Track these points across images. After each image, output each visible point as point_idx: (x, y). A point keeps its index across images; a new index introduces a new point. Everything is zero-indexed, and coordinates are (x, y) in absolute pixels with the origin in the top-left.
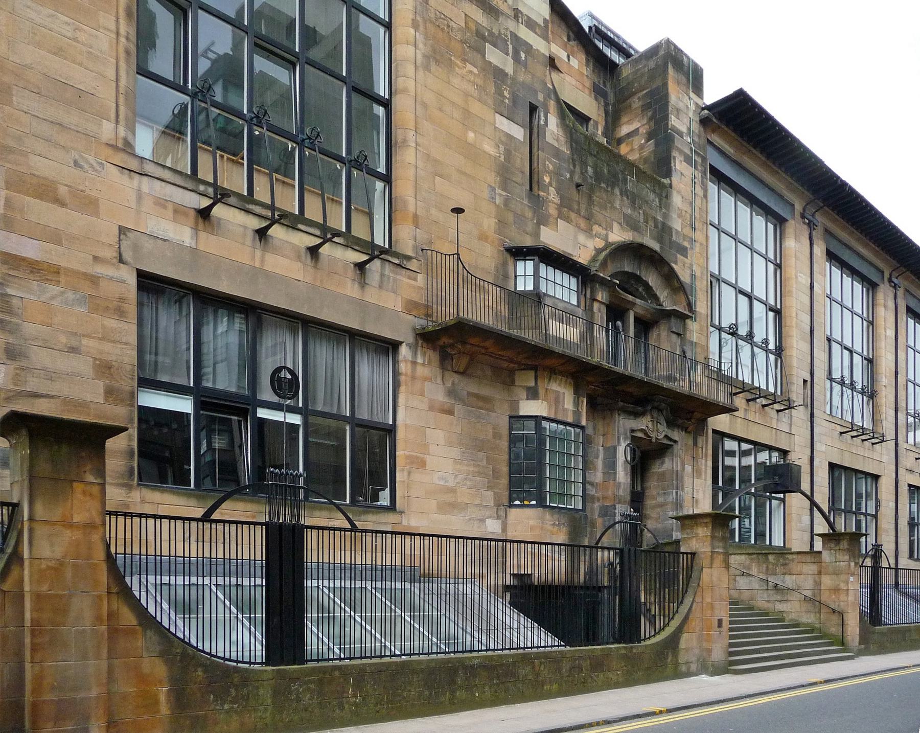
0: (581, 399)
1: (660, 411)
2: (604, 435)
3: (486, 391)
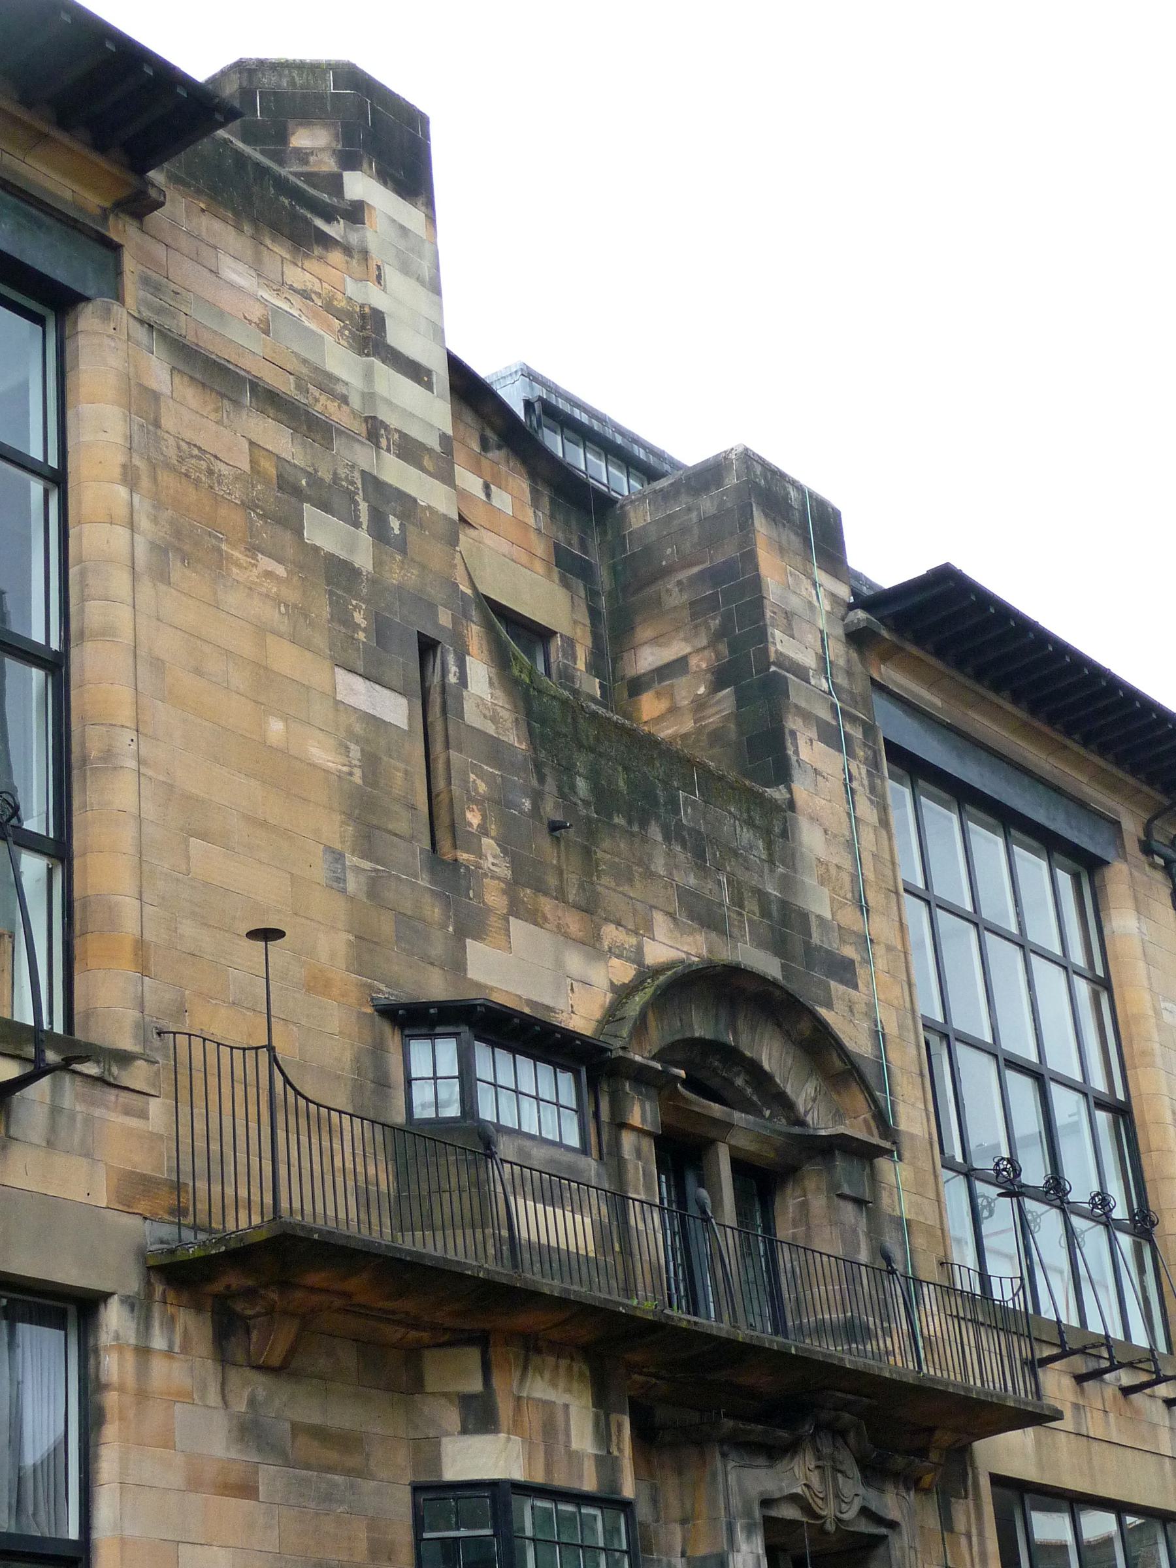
1: (839, 1433)
2: (684, 1521)
3: (344, 1416)
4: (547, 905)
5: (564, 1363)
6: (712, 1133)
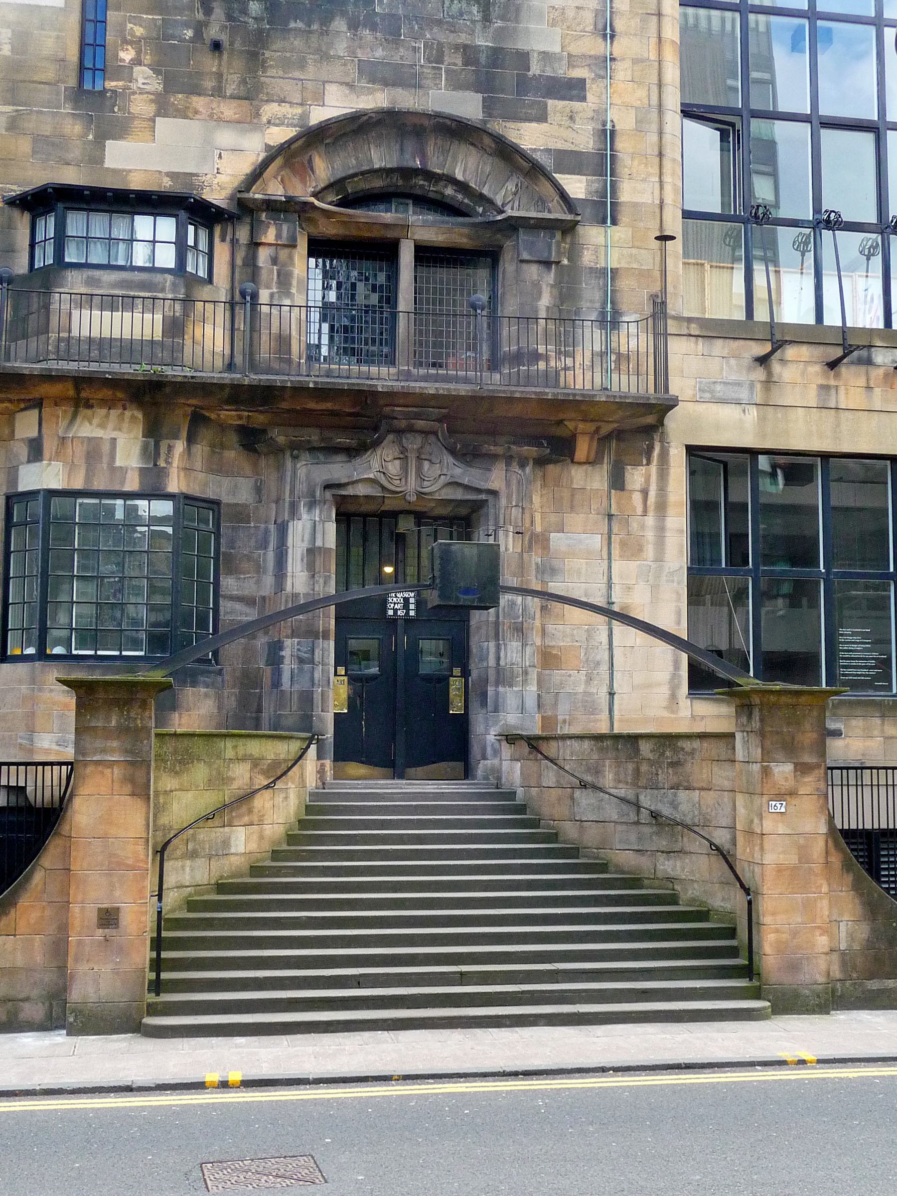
1: (425, 433)
2: (277, 502)
4: (199, 102)
6: (390, 234)
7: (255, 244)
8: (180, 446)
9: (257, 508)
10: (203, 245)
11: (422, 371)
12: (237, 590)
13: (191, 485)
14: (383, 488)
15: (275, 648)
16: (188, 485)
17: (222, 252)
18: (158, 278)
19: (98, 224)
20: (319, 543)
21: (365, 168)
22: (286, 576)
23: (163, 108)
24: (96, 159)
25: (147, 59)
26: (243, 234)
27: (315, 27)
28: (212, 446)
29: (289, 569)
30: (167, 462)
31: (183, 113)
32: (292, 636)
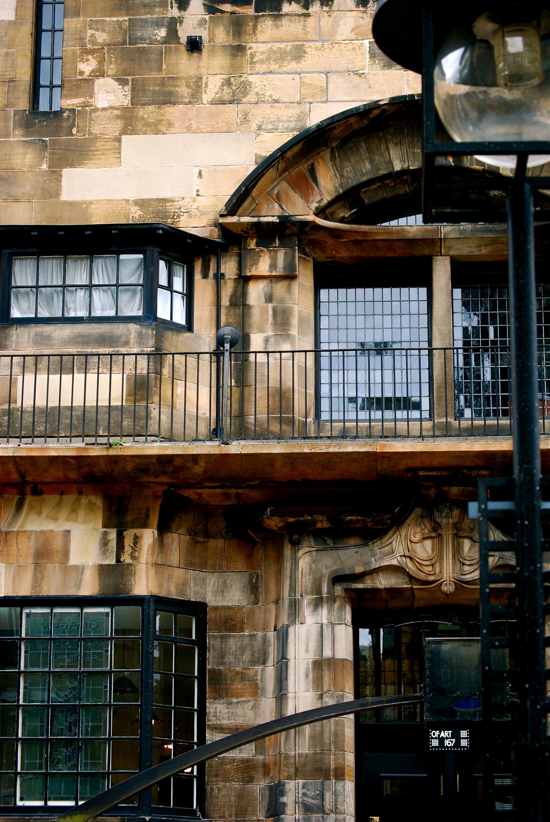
0: (129, 535)
5: (69, 498)
7: (244, 280)
8: (148, 536)
9: (253, 611)
10: (178, 284)
11: (491, 422)
12: (229, 719)
13: (165, 584)
14: (411, 578)
15: (276, 791)
16: (160, 586)
17: (204, 289)
18: (119, 329)
19: (51, 270)
20: (327, 653)
21: (383, 172)
22: (287, 698)
23: (129, 122)
24: (51, 190)
25: (111, 68)
26: (229, 268)
27: (315, 8)
28: (192, 533)
29: (291, 688)
30: (133, 557)
31: (156, 128)
32: (296, 775)
